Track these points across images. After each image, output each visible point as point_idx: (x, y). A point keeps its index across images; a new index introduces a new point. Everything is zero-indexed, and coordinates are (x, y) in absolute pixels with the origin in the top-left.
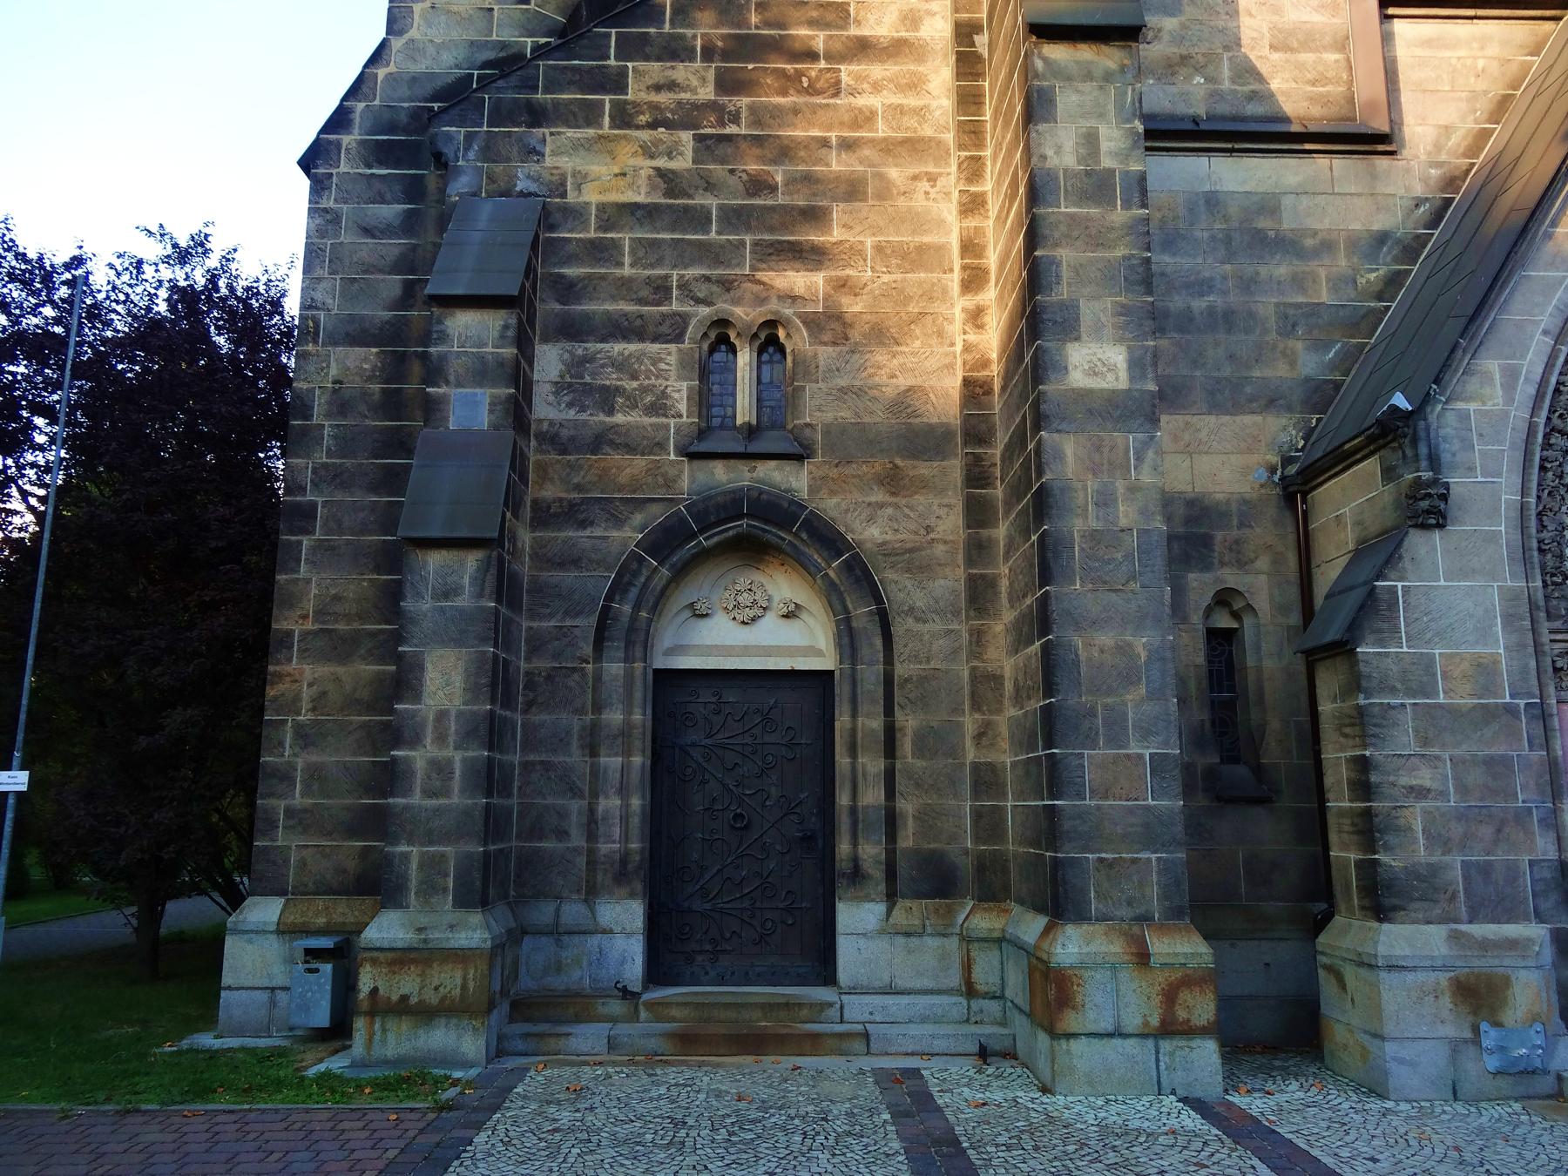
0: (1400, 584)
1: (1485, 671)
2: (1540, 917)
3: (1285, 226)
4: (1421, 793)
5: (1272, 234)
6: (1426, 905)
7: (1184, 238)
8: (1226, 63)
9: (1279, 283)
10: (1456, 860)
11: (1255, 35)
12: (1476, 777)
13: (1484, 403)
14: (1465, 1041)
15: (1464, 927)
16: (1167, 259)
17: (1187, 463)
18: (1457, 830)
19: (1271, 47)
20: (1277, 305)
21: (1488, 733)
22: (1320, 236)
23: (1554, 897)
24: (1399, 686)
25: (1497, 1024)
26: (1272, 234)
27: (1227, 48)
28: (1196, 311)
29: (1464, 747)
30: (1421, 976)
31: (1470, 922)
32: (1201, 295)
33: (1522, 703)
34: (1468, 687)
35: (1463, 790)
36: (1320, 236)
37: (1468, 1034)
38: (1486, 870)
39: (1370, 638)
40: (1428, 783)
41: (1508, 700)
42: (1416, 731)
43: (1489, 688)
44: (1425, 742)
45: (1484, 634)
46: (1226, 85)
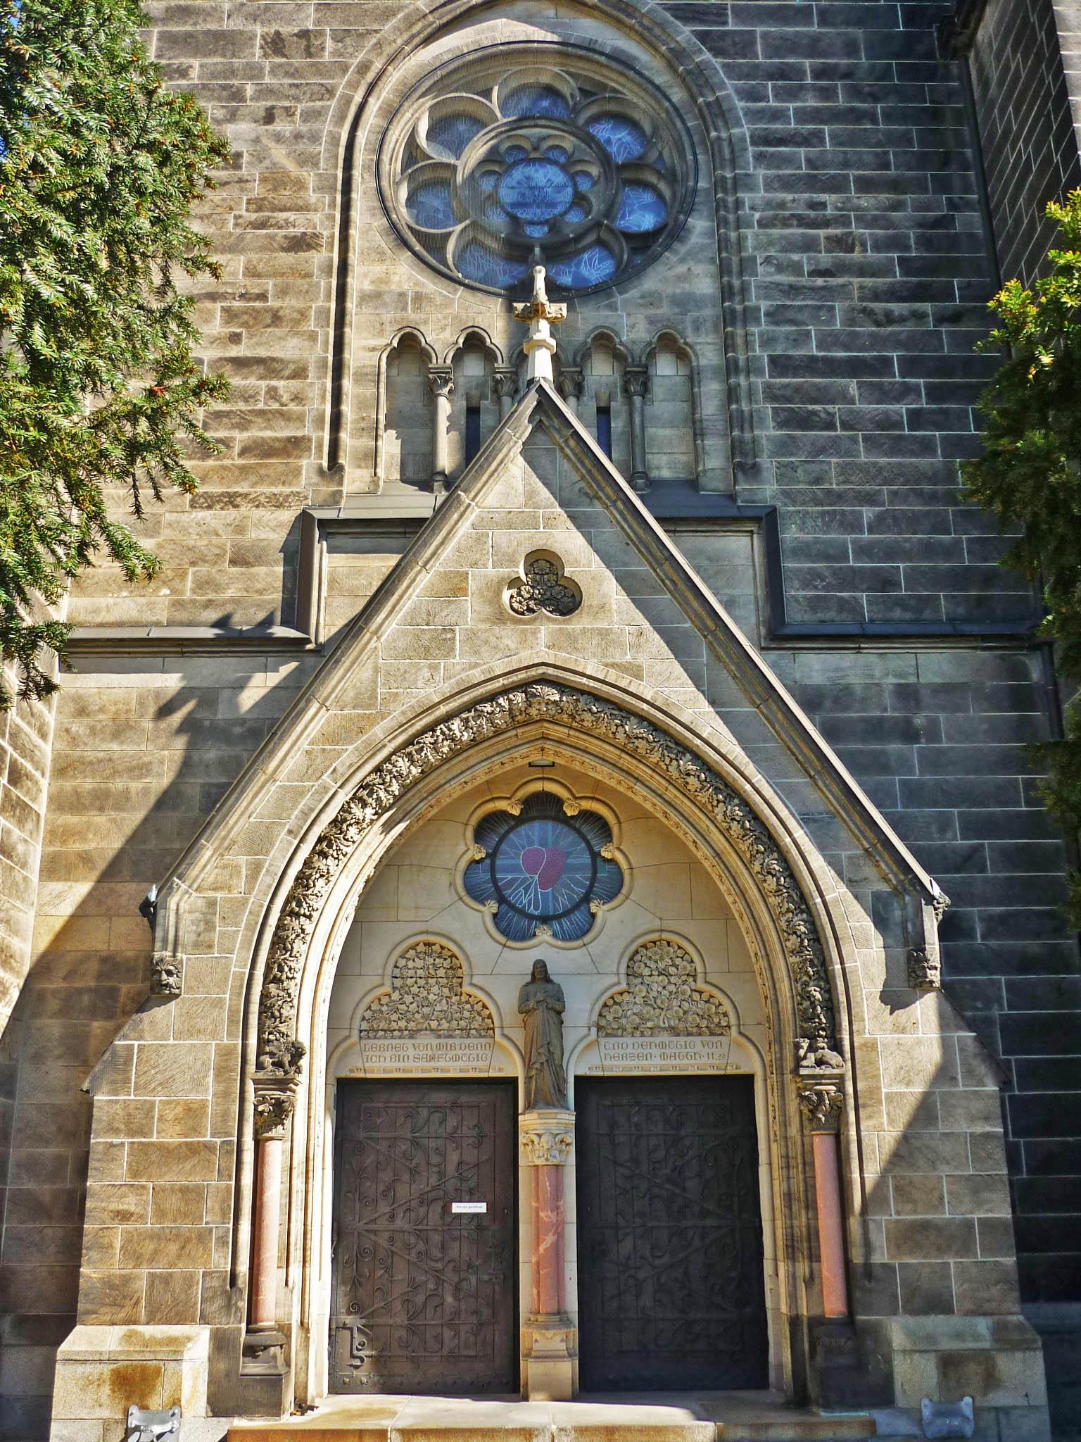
0: (136, 1043)
1: (193, 1113)
2: (205, 1320)
3: (220, 716)
4: (124, 1216)
5: (207, 723)
6: (114, 1309)
7: (132, 728)
8: (190, 577)
9: (207, 766)
10: (144, 1271)
11: (218, 551)
12: (173, 1202)
13: (230, 891)
14: (116, 1421)
15: (139, 1328)
16: (115, 746)
17: (107, 925)
18: (149, 1247)
19: (231, 561)
20: (203, 785)
21: (188, 1166)
22: (247, 725)
23: (218, 1303)
24: (122, 1127)
25: (144, 1407)
26: (207, 723)
27: (193, 564)
28: (133, 791)
29: (167, 1178)
30: (89, 1368)
31: (148, 1323)
32: (140, 777)
33: (218, 1141)
34: (178, 1128)
35: (160, 1214)
36: (247, 725)
37: (120, 1416)
38: (167, 1280)
39: (105, 1088)
40: (132, 1209)
41: (208, 1139)
42: (129, 1164)
43: (195, 1130)
44: (135, 1174)
45: (198, 1083)
46: (188, 595)
